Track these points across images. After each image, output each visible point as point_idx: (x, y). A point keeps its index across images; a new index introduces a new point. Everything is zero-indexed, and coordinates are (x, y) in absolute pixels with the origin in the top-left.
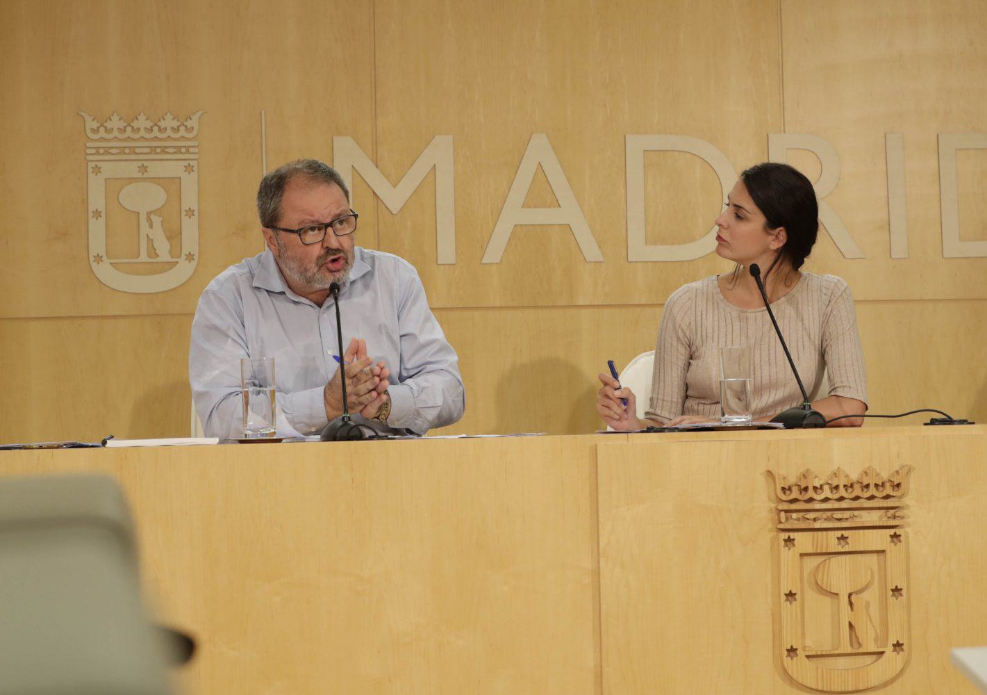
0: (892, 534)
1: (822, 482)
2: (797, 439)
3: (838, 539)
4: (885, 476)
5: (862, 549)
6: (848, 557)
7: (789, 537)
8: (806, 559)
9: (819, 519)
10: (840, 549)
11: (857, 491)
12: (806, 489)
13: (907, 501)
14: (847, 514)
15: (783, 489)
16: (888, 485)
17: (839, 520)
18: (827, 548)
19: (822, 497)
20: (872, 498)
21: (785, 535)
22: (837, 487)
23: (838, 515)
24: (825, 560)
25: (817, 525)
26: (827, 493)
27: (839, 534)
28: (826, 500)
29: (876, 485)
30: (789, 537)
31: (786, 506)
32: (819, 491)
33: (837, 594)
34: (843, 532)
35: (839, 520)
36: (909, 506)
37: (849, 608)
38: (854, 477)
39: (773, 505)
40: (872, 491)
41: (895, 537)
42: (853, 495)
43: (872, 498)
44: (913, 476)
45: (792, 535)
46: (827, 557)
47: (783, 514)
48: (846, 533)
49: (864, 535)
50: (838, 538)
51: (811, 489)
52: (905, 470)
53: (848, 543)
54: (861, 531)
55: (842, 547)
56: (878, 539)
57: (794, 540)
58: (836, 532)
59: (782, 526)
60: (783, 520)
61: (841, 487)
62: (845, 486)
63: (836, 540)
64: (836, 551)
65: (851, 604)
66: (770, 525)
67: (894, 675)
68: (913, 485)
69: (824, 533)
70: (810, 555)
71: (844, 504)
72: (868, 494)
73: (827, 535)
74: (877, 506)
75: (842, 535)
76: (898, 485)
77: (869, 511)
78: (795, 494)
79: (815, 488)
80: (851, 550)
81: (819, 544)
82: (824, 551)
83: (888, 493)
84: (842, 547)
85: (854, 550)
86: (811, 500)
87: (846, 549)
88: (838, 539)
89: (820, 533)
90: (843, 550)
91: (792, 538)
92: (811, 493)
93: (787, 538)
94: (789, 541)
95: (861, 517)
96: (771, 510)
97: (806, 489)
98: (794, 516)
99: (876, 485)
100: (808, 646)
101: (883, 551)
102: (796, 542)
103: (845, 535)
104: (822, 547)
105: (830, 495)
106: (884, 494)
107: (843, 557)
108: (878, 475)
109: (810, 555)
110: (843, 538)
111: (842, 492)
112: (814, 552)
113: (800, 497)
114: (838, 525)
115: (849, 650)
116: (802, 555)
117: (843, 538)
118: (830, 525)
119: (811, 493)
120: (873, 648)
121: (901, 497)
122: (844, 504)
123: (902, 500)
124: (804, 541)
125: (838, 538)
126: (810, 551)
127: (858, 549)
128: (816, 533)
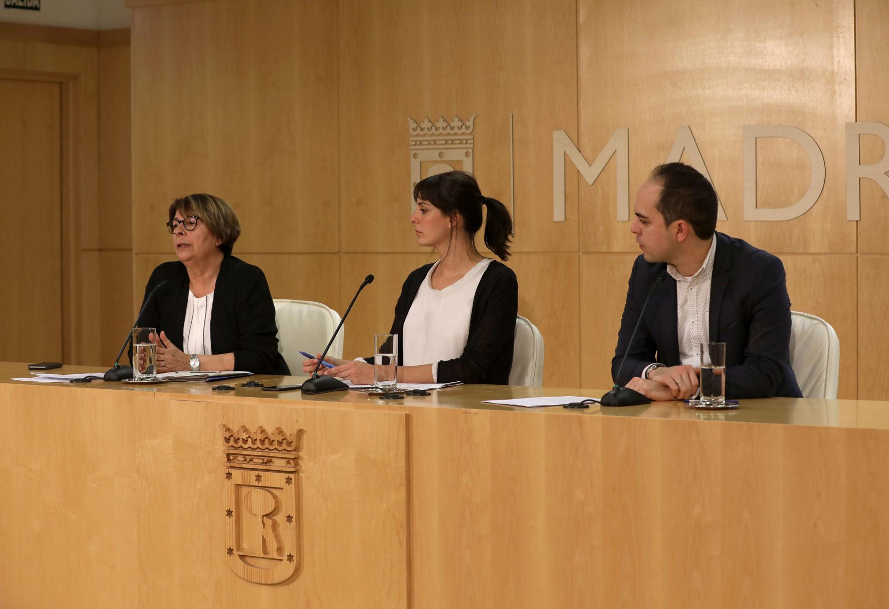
1: (247, 436)
2: (239, 404)
10: (256, 484)
13: (301, 454)
15: (227, 440)
23: (255, 460)
25: (244, 466)
26: (249, 444)
27: (256, 473)
33: (256, 515)
34: (259, 472)
36: (303, 458)
37: (262, 525)
41: (289, 480)
44: (305, 437)
45: (232, 471)
48: (261, 473)
56: (277, 480)
57: (231, 474)
64: (255, 485)
65: (263, 523)
67: (288, 577)
73: (271, 474)
76: (292, 442)
82: (248, 484)
83: (285, 448)
87: (260, 484)
90: (259, 485)
92: (241, 443)
94: (229, 475)
100: (245, 549)
104: (247, 482)
105: (251, 446)
112: (242, 484)
114: (256, 467)
115: (262, 555)
116: (238, 486)
118: (252, 467)
119: (241, 443)
120: (276, 556)
127: (267, 486)
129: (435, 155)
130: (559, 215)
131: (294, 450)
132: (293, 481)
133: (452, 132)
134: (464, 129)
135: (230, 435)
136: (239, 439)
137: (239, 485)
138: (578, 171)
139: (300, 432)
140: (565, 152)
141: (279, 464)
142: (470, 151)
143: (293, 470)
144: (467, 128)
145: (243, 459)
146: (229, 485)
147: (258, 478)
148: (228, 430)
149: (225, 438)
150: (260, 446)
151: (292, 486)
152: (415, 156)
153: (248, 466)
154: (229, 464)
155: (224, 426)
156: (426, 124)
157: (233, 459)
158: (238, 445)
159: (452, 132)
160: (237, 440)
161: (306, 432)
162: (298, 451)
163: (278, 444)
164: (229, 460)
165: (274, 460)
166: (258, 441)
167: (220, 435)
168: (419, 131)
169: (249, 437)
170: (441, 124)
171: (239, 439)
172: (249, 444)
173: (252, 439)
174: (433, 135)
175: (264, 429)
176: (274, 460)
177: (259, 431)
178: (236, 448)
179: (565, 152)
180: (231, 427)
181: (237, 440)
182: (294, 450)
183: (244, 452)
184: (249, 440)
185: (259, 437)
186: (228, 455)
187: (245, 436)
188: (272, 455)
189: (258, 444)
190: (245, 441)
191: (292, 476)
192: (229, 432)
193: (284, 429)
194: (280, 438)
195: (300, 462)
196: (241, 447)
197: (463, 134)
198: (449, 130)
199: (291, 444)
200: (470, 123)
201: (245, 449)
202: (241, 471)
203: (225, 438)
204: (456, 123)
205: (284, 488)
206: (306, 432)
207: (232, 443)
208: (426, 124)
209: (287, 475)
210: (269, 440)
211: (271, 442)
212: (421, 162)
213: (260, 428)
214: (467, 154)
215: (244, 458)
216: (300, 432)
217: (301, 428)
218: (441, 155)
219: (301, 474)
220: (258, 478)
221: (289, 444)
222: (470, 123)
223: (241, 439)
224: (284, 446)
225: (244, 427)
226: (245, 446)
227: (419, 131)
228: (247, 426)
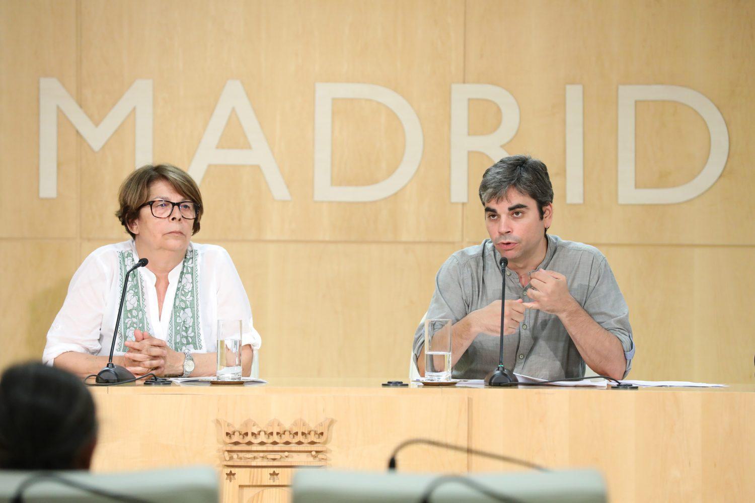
1: (259, 430)
3: (270, 474)
4: (312, 426)
6: (278, 489)
7: (231, 472)
8: (246, 490)
9: (257, 458)
10: (272, 483)
11: (287, 437)
12: (246, 434)
13: (329, 446)
14: (277, 456)
15: (227, 434)
16: (312, 433)
17: (274, 459)
18: (261, 481)
19: (259, 440)
20: (300, 443)
21: (228, 470)
22: (272, 434)
24: (259, 492)
25: (254, 463)
26: (262, 438)
27: (271, 470)
28: (262, 443)
29: (303, 434)
30: (231, 472)
31: (229, 448)
32: (258, 436)
34: (275, 469)
35: (274, 459)
36: (331, 451)
38: (287, 425)
39: (221, 446)
40: (300, 438)
42: (284, 440)
43: (249, 443)
44: (335, 427)
45: (234, 470)
46: (262, 488)
47: (226, 453)
48: (277, 470)
49: (261, 472)
50: (270, 474)
51: (250, 434)
52: (328, 422)
53: (278, 479)
55: (274, 482)
58: (269, 469)
59: (226, 463)
60: (228, 458)
61: (275, 434)
62: (278, 433)
63: (269, 475)
64: (269, 484)
66: (218, 462)
68: (335, 433)
69: (260, 469)
70: (249, 486)
71: (276, 448)
72: (271, 440)
74: (303, 450)
76: (322, 434)
77: (299, 454)
78: (236, 438)
79: (253, 434)
80: (280, 484)
81: (255, 479)
82: (259, 484)
83: (312, 440)
84: (274, 482)
85: (283, 484)
86: (249, 443)
88: (270, 474)
89: (256, 469)
90: (274, 484)
91: (233, 472)
92: (250, 438)
93: (229, 472)
95: (292, 457)
96: (219, 450)
97: (246, 434)
98: (235, 456)
99: (278, 433)
102: (236, 476)
103: (277, 472)
104: (257, 480)
105: (265, 440)
106: (310, 441)
107: (274, 489)
109: (249, 486)
110: (274, 474)
111: (275, 438)
112: (250, 484)
113: (241, 441)
116: (240, 486)
117: (274, 474)
118: (265, 463)
121: (325, 443)
122: (276, 448)
123: (326, 446)
124: (243, 476)
125: (270, 474)
128: (252, 469)
131: (319, 443)
139: (332, 422)
153: (259, 462)
161: (336, 421)
164: (231, 458)
177: (276, 424)
182: (319, 443)
183: (254, 448)
188: (293, 449)
202: (248, 470)
206: (336, 421)
216: (332, 422)
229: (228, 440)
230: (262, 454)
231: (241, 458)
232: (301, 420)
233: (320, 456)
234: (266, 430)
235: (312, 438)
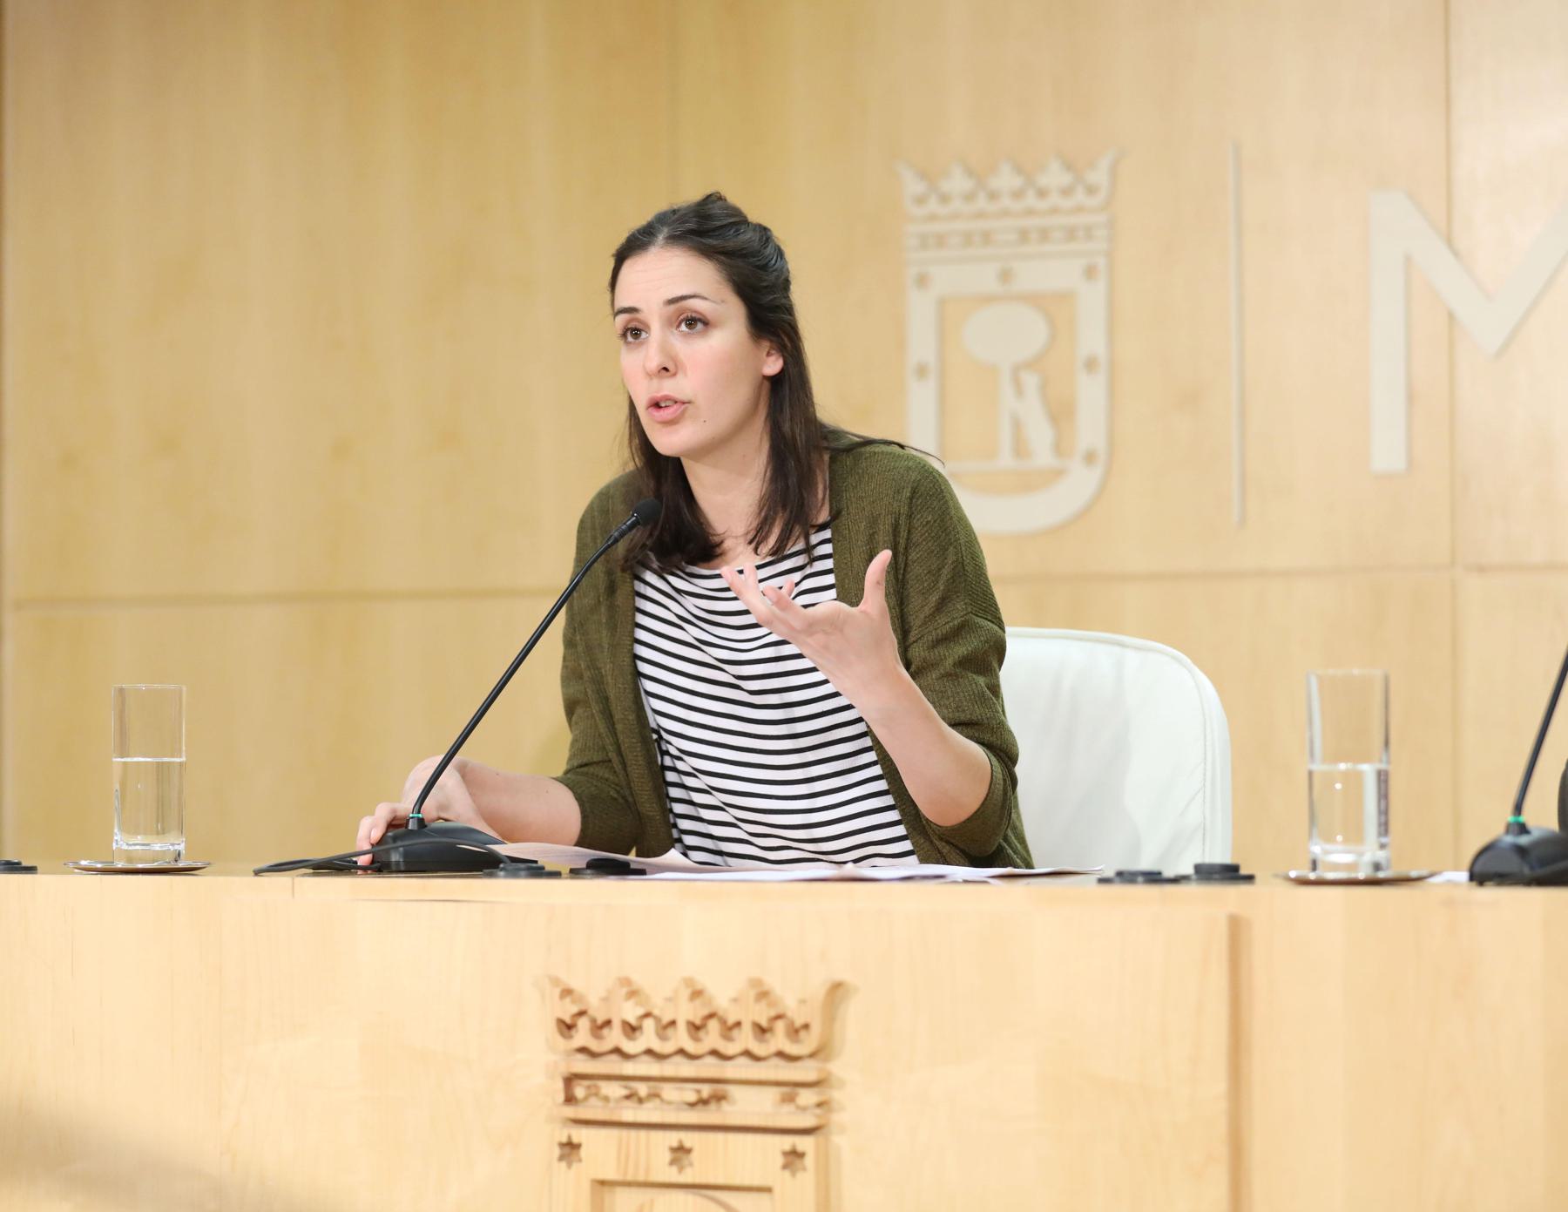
0: (787, 1148)
1: (641, 1011)
5: (721, 1181)
7: (569, 1137)
10: (672, 1175)
13: (836, 1067)
15: (567, 1027)
23: (669, 1092)
25: (630, 1114)
26: (648, 1038)
27: (673, 1138)
30: (569, 1137)
41: (794, 1156)
45: (580, 1135)
48: (689, 1139)
54: (720, 1137)
55: (681, 1169)
69: (643, 1134)
71: (686, 1069)
75: (681, 1142)
76: (806, 1026)
82: (641, 1178)
87: (688, 1177)
89: (633, 1133)
92: (615, 1037)
101: (768, 1190)
102: (583, 1152)
103: (687, 1144)
105: (657, 1046)
108: (763, 995)
113: (594, 1046)
118: (655, 1118)
119: (615, 1037)
124: (601, 1151)
126: (611, 1175)
129: (984, 278)
130: (1387, 453)
131: (812, 1055)
132: (809, 1161)
133: (1041, 205)
134: (1080, 197)
135: (575, 1009)
136: (608, 1023)
137: (603, 1183)
138: (1451, 316)
139: (837, 991)
140: (1408, 260)
141: (748, 1105)
142: (1101, 262)
143: (807, 1121)
144: (1091, 190)
145: (625, 1092)
146: (573, 1182)
147: (681, 1151)
148: (567, 992)
149: (561, 1022)
150: (691, 1047)
151: (807, 1178)
152: (922, 281)
154: (571, 1111)
155: (555, 981)
156: (957, 183)
157: (586, 1098)
158: (607, 1045)
159: (1041, 205)
160: (600, 1027)
162: (827, 1059)
163: (756, 1037)
164: (570, 1099)
165: (734, 1091)
166: (682, 1027)
167: (541, 1014)
168: (933, 205)
169: (647, 1015)
170: (1006, 180)
171: (608, 1023)
172: (648, 1038)
173: (658, 1020)
174: (980, 215)
175: (699, 987)
176: (734, 1091)
177: (685, 993)
178: (593, 1055)
179: (1408, 260)
180: (575, 984)
181: (600, 1027)
182: (812, 1055)
183: (629, 1068)
184: (649, 1024)
185: (687, 1012)
186: (570, 1080)
187: (631, 1013)
188: (730, 1070)
189: (681, 1038)
190: (631, 1029)
191: (804, 1143)
192: (573, 1002)
193: (773, 982)
194: (762, 1015)
195: (836, 1095)
196: (617, 1051)
197: (1079, 209)
198: (1031, 200)
199: (803, 1034)
200: (1099, 176)
201: (626, 1056)
202: (614, 1133)
203: (561, 1022)
204: (1054, 177)
205: (777, 1191)
207: (582, 1036)
208: (957, 183)
209: (787, 1142)
210: (723, 1022)
211: (730, 1029)
212: (942, 303)
213: (689, 982)
214: (1090, 272)
215: (626, 1087)
216: (837, 991)
217: (839, 976)
218: (1005, 276)
219: (837, 1139)
220: (681, 1151)
221: (795, 1032)
222: (1099, 176)
223: (616, 1024)
224: (779, 1041)
225: (626, 981)
226: (630, 1047)
227: (933, 205)
228: (638, 979)
229: (562, 1043)
230: (642, 1089)
231: (606, 1099)
232: (756, 983)
233: (807, 1097)
234: (656, 1012)
235: (779, 1041)
